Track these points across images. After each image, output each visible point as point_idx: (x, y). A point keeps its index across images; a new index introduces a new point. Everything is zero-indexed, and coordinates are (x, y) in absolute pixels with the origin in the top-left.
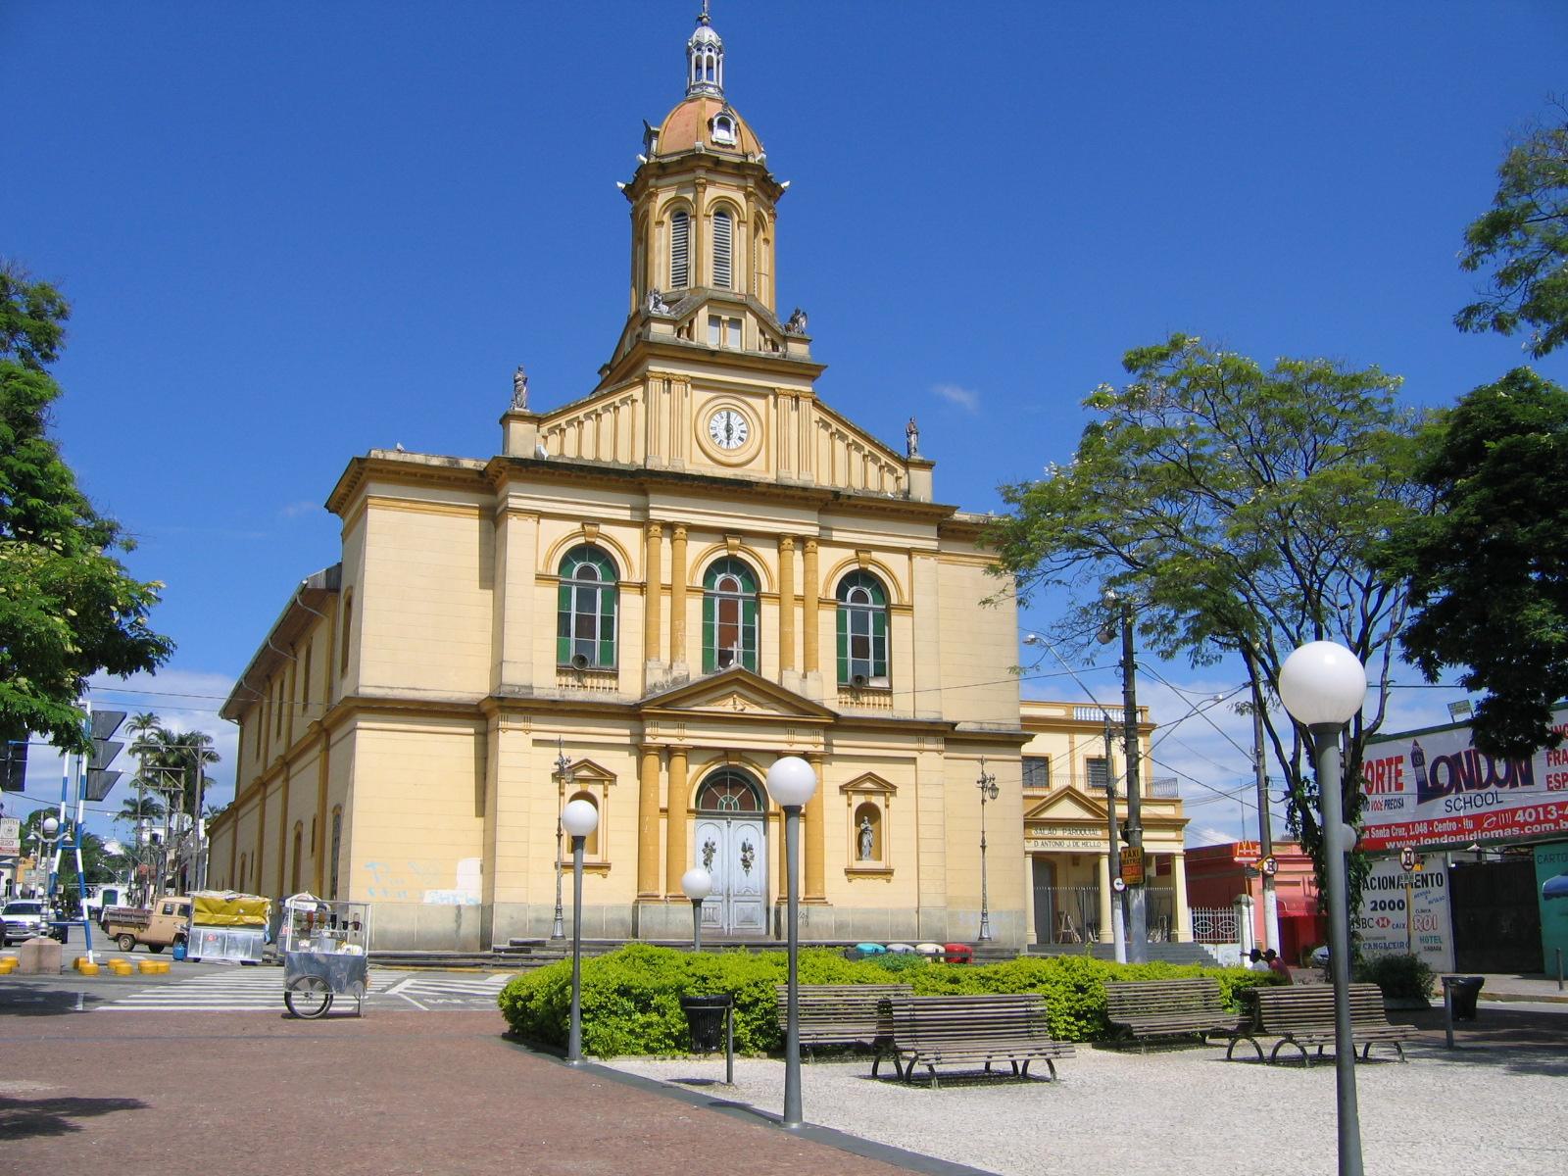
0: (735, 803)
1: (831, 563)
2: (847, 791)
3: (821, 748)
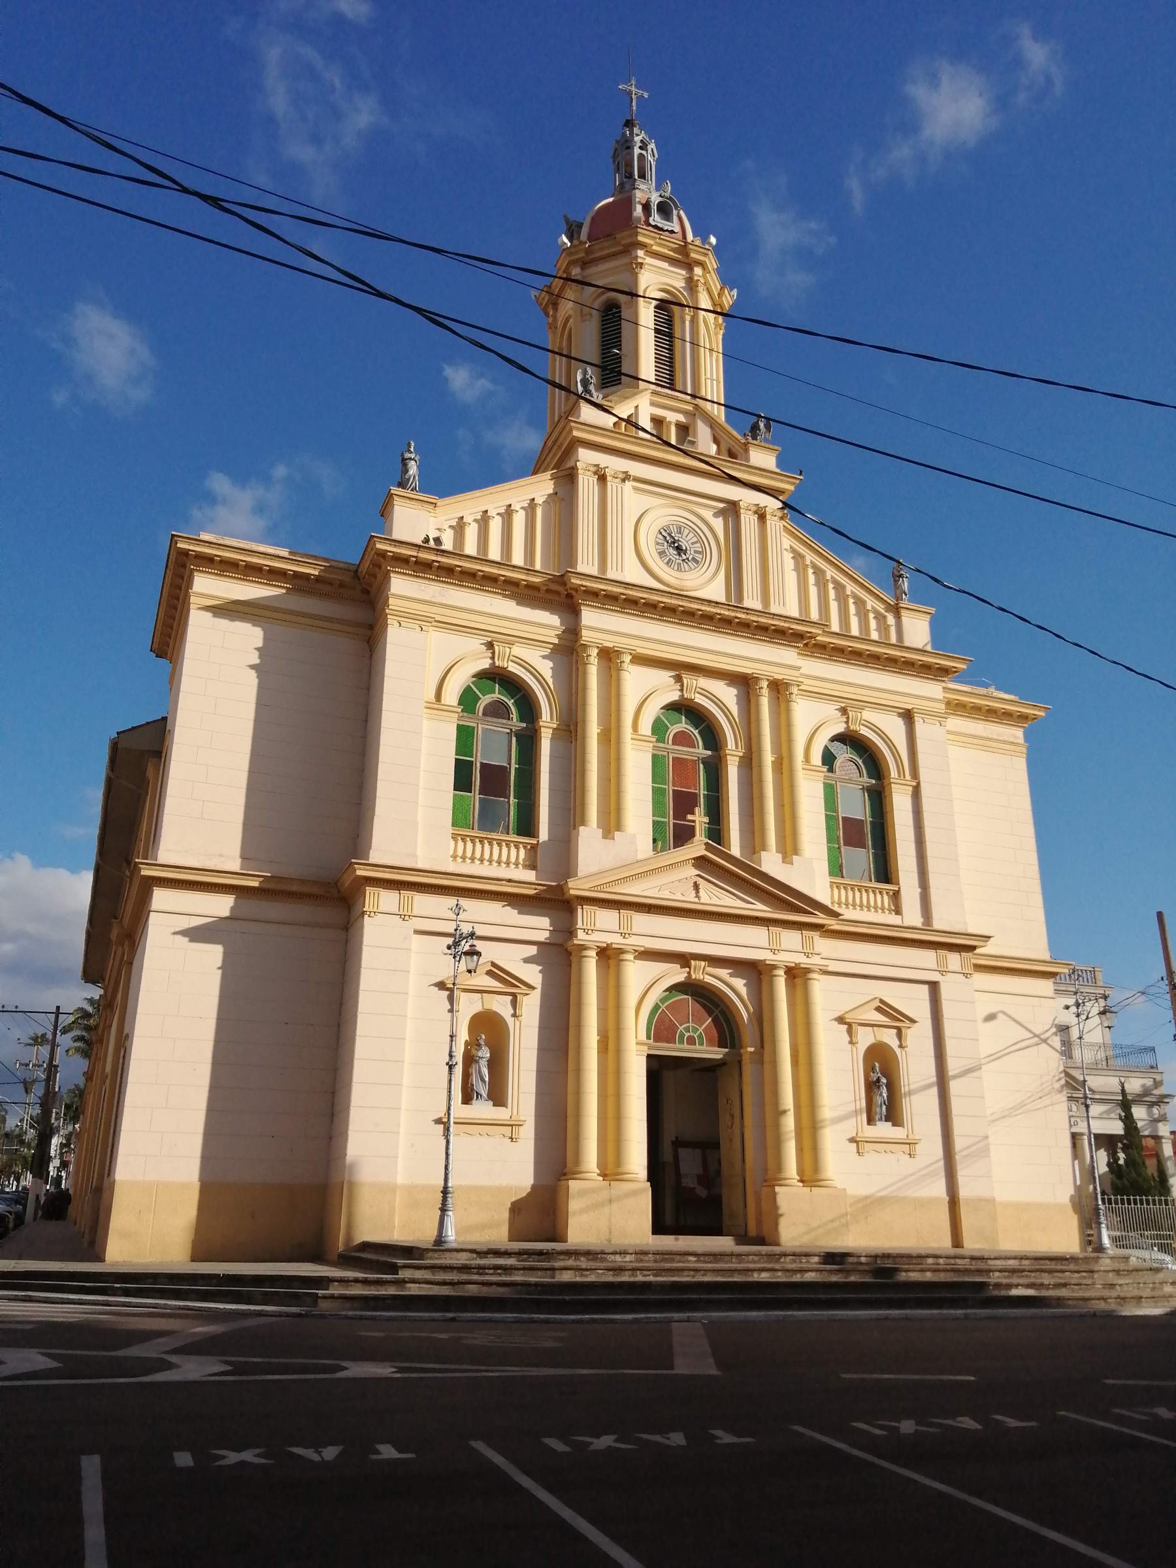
0: (700, 1036)
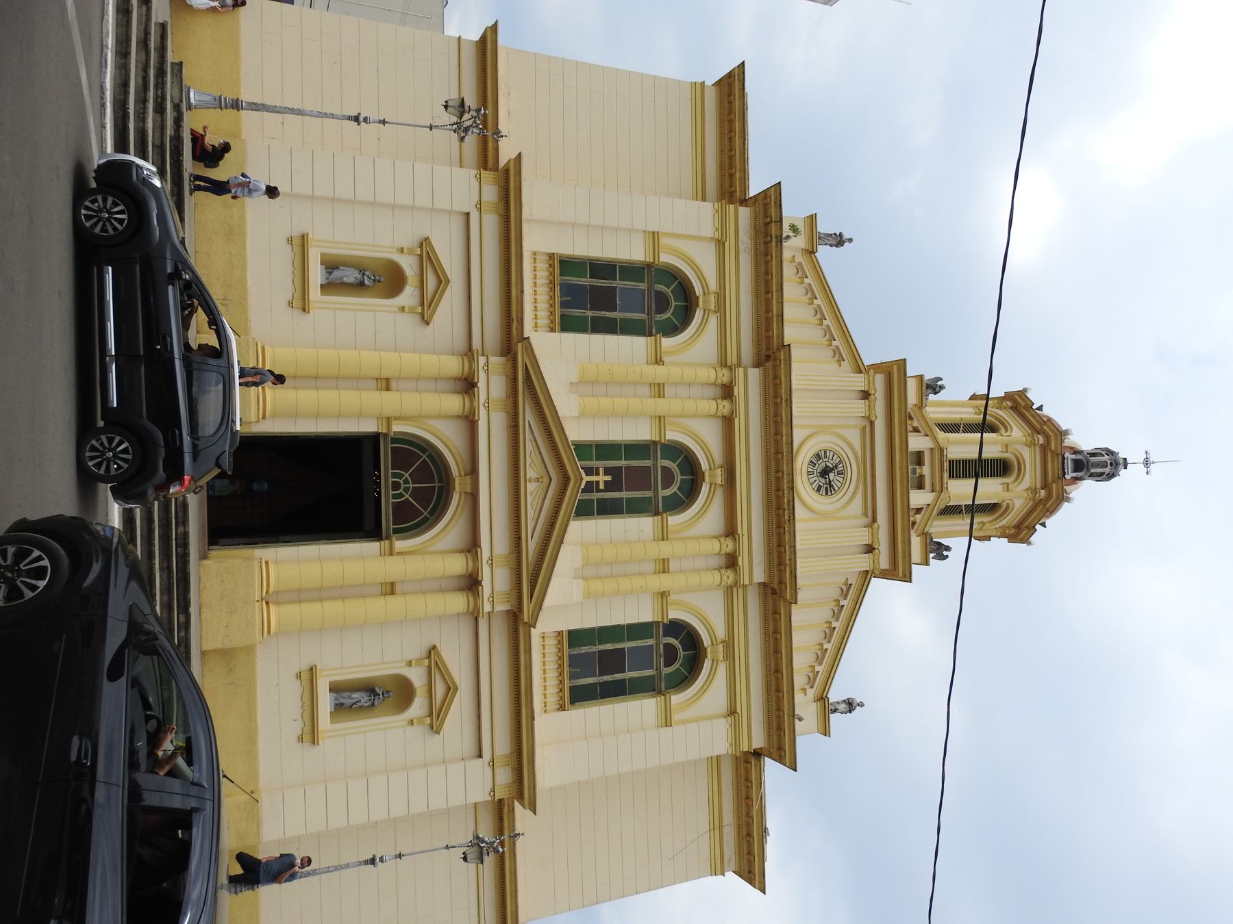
0: (401, 495)
1: (705, 610)
2: (429, 657)
3: (487, 608)
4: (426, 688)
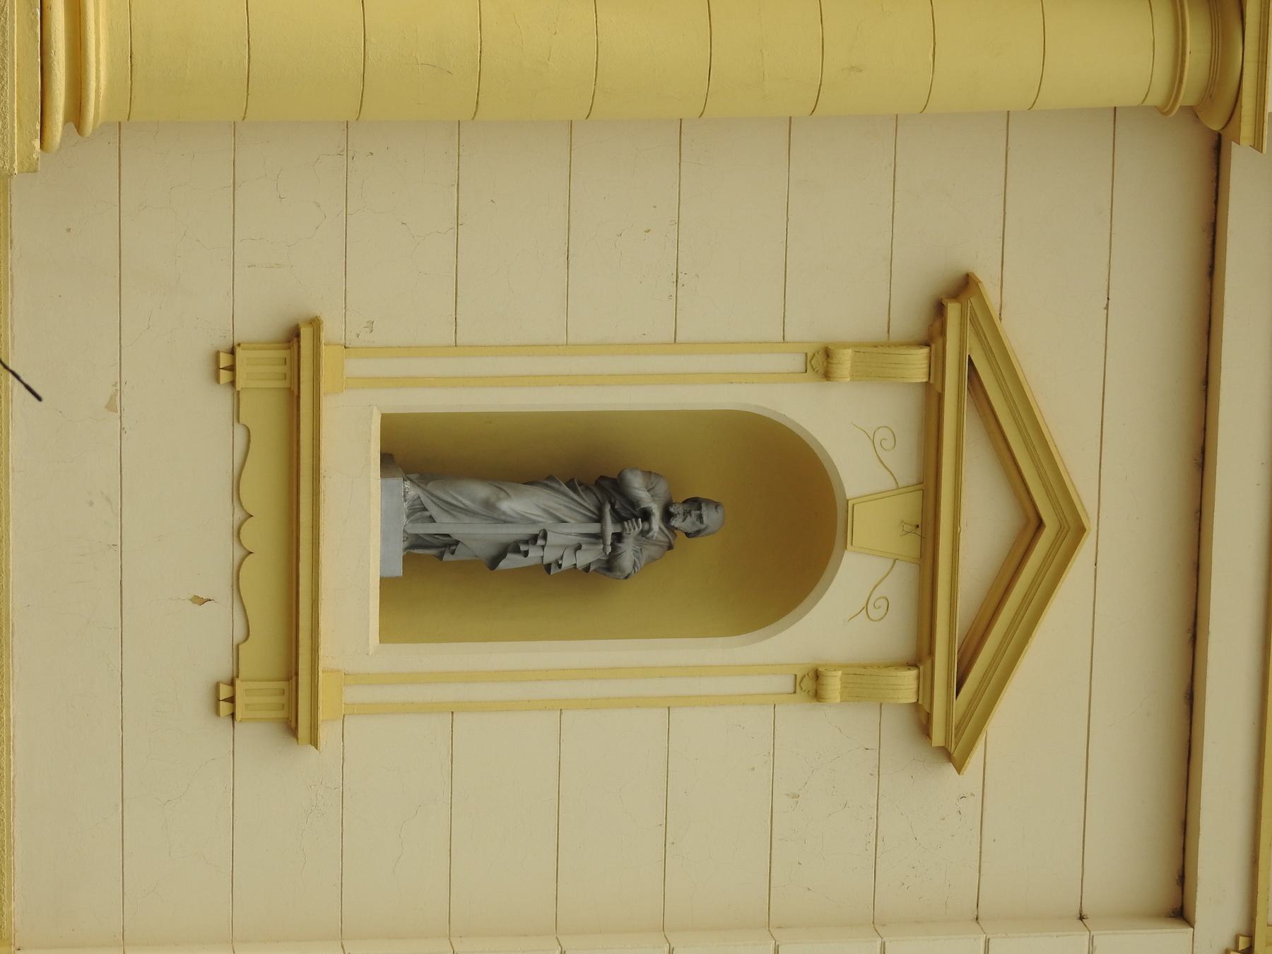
2: (932, 337)
4: (906, 507)
